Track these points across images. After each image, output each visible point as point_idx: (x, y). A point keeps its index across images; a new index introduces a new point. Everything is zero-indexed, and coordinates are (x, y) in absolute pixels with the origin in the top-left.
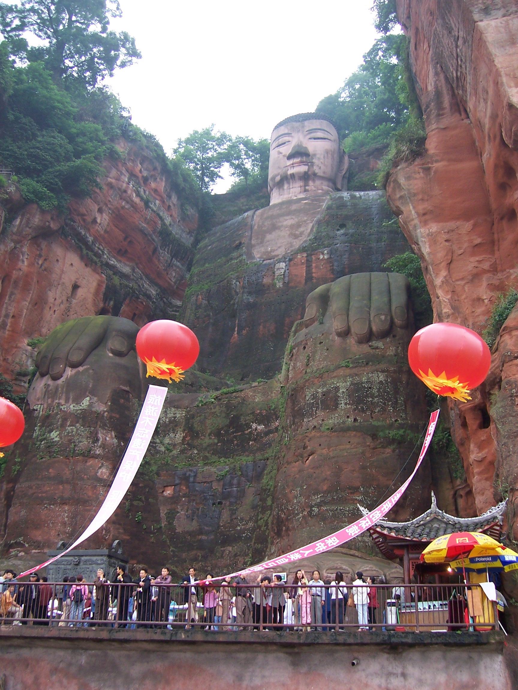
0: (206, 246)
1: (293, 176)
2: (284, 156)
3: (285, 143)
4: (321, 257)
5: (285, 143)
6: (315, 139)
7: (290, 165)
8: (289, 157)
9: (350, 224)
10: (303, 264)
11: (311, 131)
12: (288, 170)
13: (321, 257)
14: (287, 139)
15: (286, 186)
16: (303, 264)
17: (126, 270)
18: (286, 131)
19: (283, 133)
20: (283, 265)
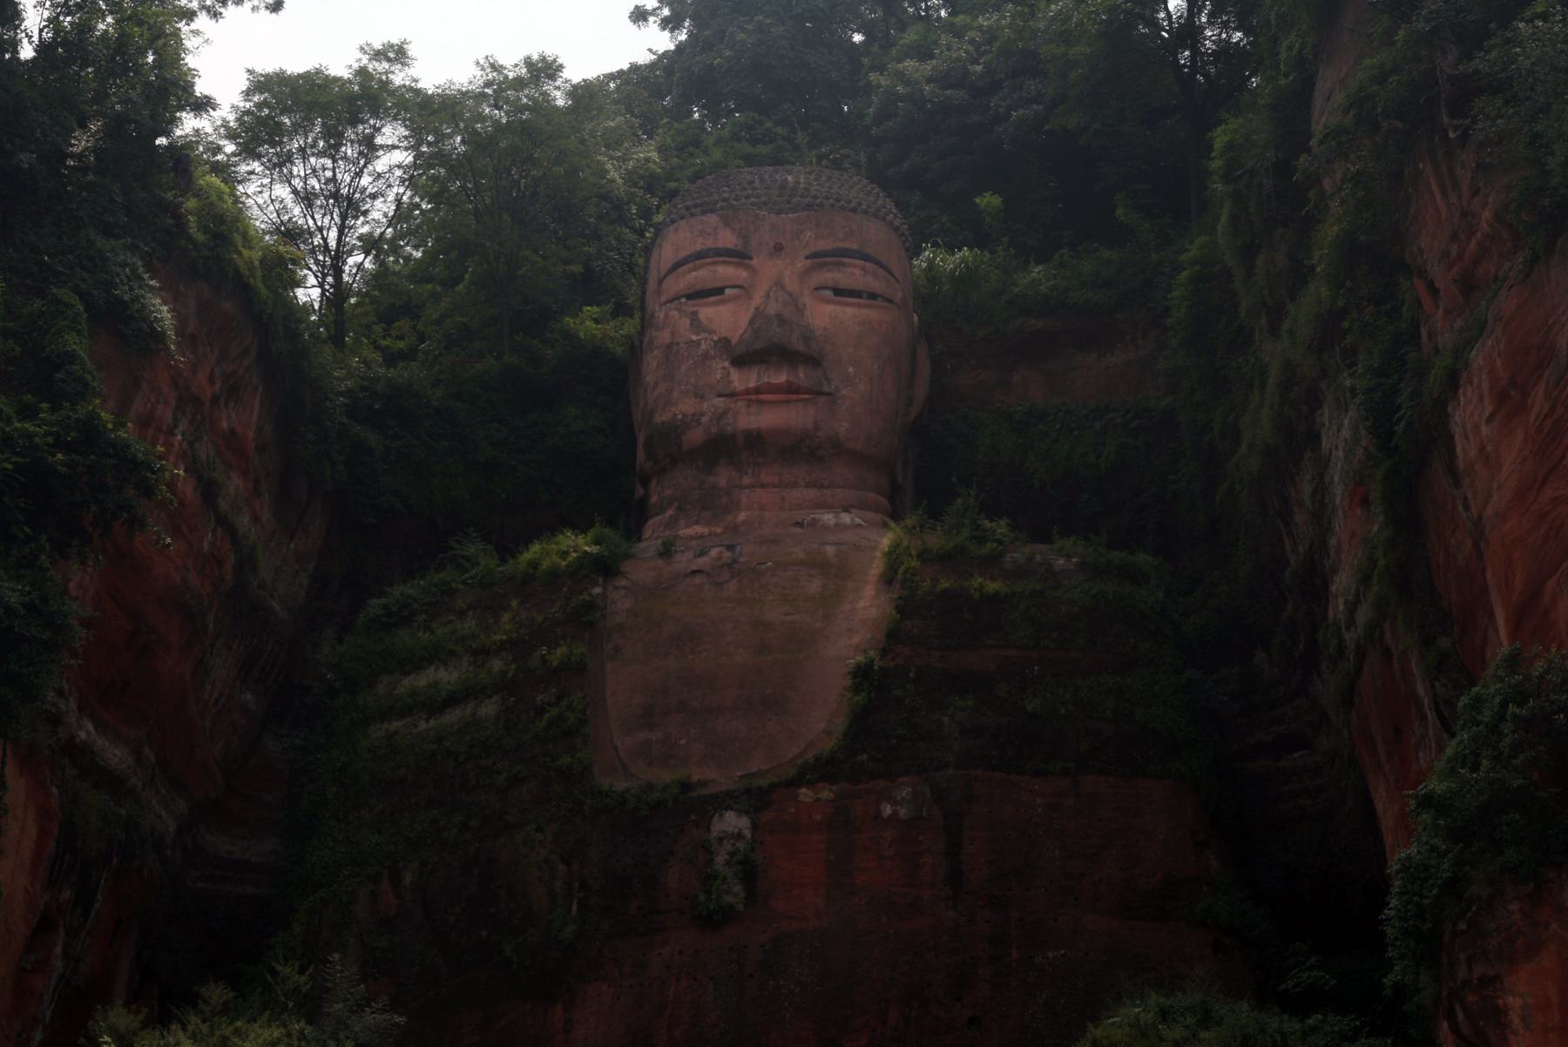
0: (437, 704)
1: (756, 442)
4: (887, 810)
5: (719, 291)
7: (748, 392)
11: (821, 259)
13: (887, 810)
14: (726, 272)
17: (115, 755)
18: (727, 239)
20: (732, 822)
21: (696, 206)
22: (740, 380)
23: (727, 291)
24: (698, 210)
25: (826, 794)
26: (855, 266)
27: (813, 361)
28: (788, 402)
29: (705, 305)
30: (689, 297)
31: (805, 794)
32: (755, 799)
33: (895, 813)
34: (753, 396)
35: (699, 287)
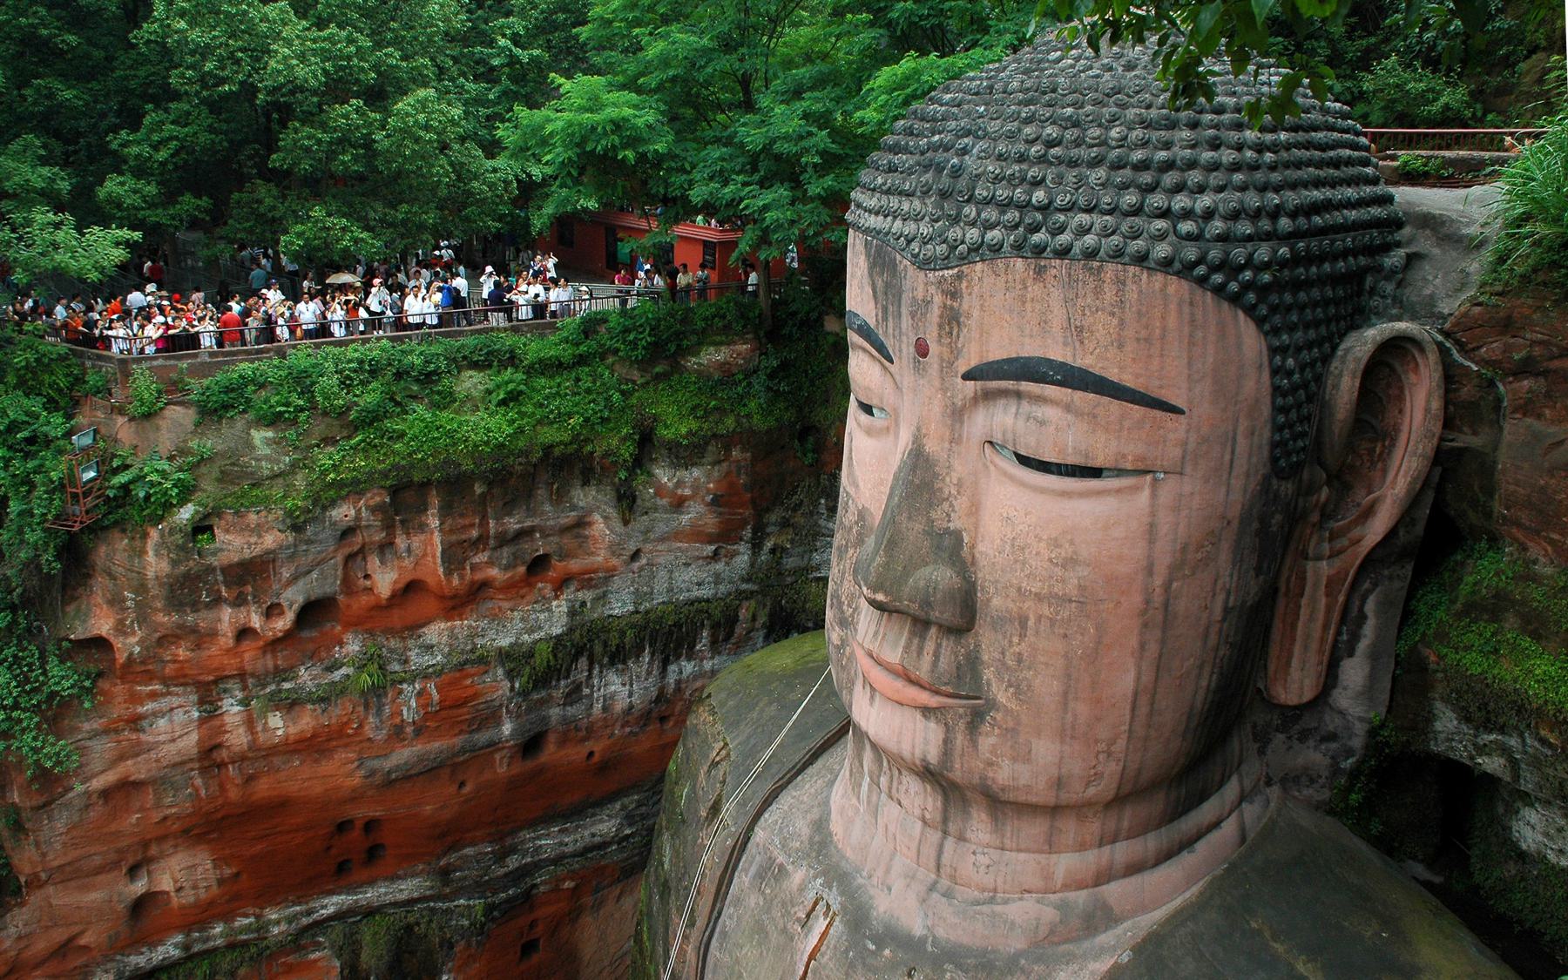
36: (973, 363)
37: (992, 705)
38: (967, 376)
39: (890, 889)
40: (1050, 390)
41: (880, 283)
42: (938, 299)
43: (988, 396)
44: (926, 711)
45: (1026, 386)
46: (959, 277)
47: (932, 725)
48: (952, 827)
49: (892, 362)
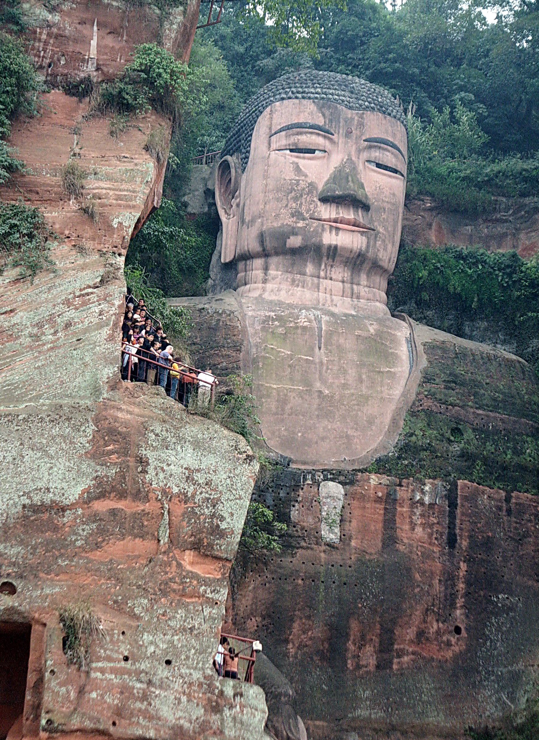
1: (333, 252)
2: (312, 186)
3: (312, 151)
5: (312, 151)
6: (379, 165)
8: (325, 200)
9: (469, 434)
10: (378, 500)
12: (323, 230)
15: (310, 268)
16: (378, 500)
18: (320, 121)
19: (311, 121)
21: (298, 92)
22: (327, 212)
23: (317, 152)
24: (300, 96)
25: (385, 479)
26: (389, 151)
27: (366, 208)
28: (354, 231)
29: (304, 158)
30: (291, 150)
31: (374, 480)
32: (347, 478)
33: (422, 499)
34: (336, 224)
35: (301, 146)
36: (368, 137)
37: (379, 232)
38: (364, 141)
39: (336, 305)
40: (389, 148)
41: (327, 113)
42: (356, 118)
43: (370, 147)
44: (362, 233)
45: (382, 145)
46: (363, 114)
47: (364, 238)
48: (355, 281)
49: (333, 135)
